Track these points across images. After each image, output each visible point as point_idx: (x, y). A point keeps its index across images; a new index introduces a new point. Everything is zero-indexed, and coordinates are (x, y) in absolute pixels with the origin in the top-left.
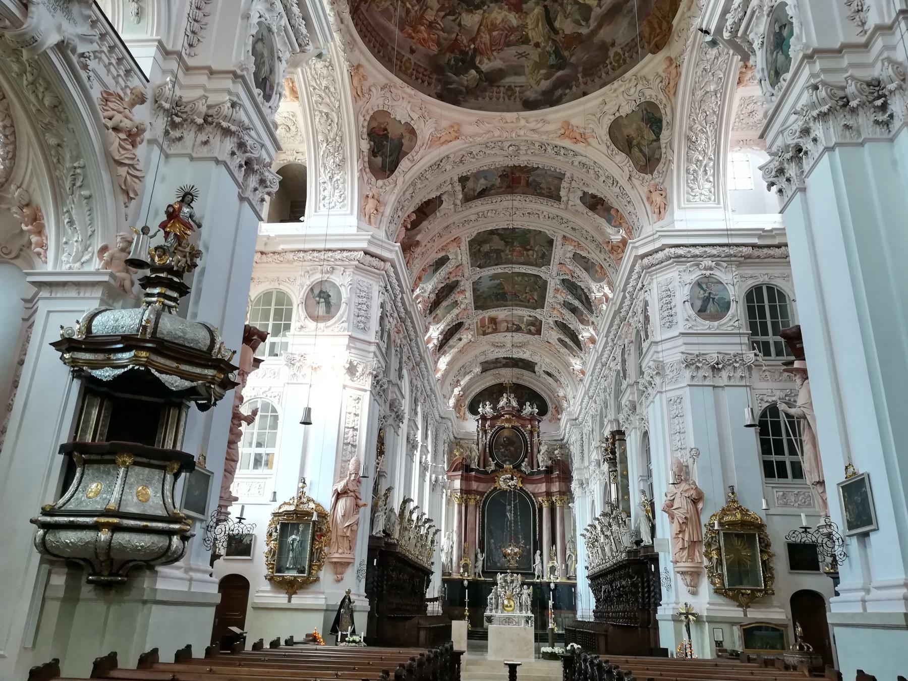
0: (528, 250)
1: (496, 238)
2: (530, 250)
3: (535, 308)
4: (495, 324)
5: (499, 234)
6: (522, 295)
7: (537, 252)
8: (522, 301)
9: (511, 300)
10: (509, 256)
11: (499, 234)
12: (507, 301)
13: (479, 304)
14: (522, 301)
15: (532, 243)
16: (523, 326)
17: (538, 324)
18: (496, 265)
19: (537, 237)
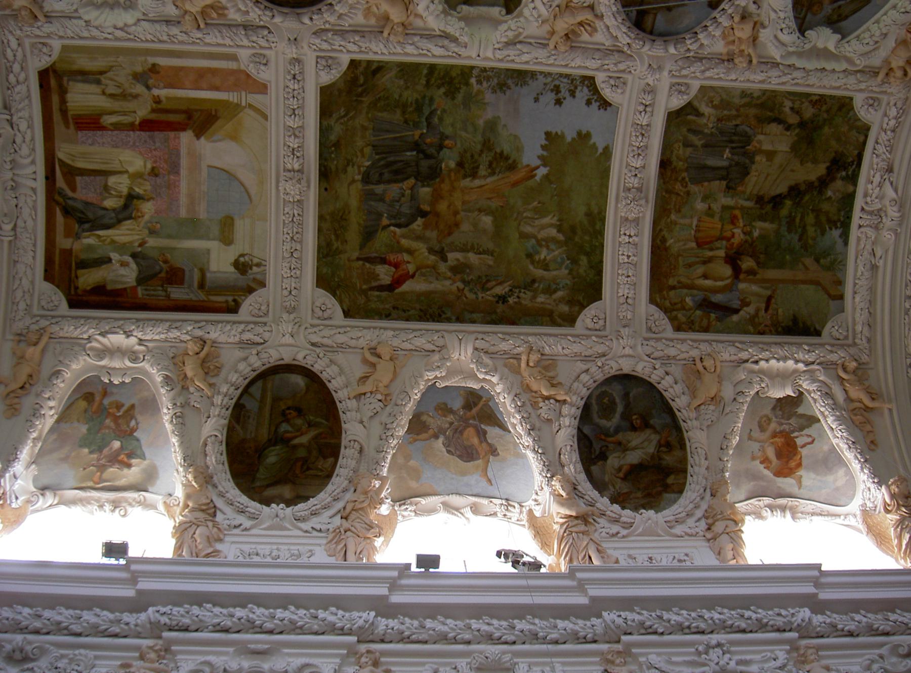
0: (732, 260)
1: (815, 172)
2: (737, 271)
3: (322, 281)
4: (147, 125)
5: (823, 183)
6: (418, 238)
7: (729, 288)
8: (368, 235)
9: (369, 196)
10: (700, 206)
11: (823, 183)
12: (366, 179)
13: (386, 80)
14: (368, 235)
15: (772, 274)
16: (125, 234)
17: (177, 293)
18: (664, 164)
19: (810, 291)
